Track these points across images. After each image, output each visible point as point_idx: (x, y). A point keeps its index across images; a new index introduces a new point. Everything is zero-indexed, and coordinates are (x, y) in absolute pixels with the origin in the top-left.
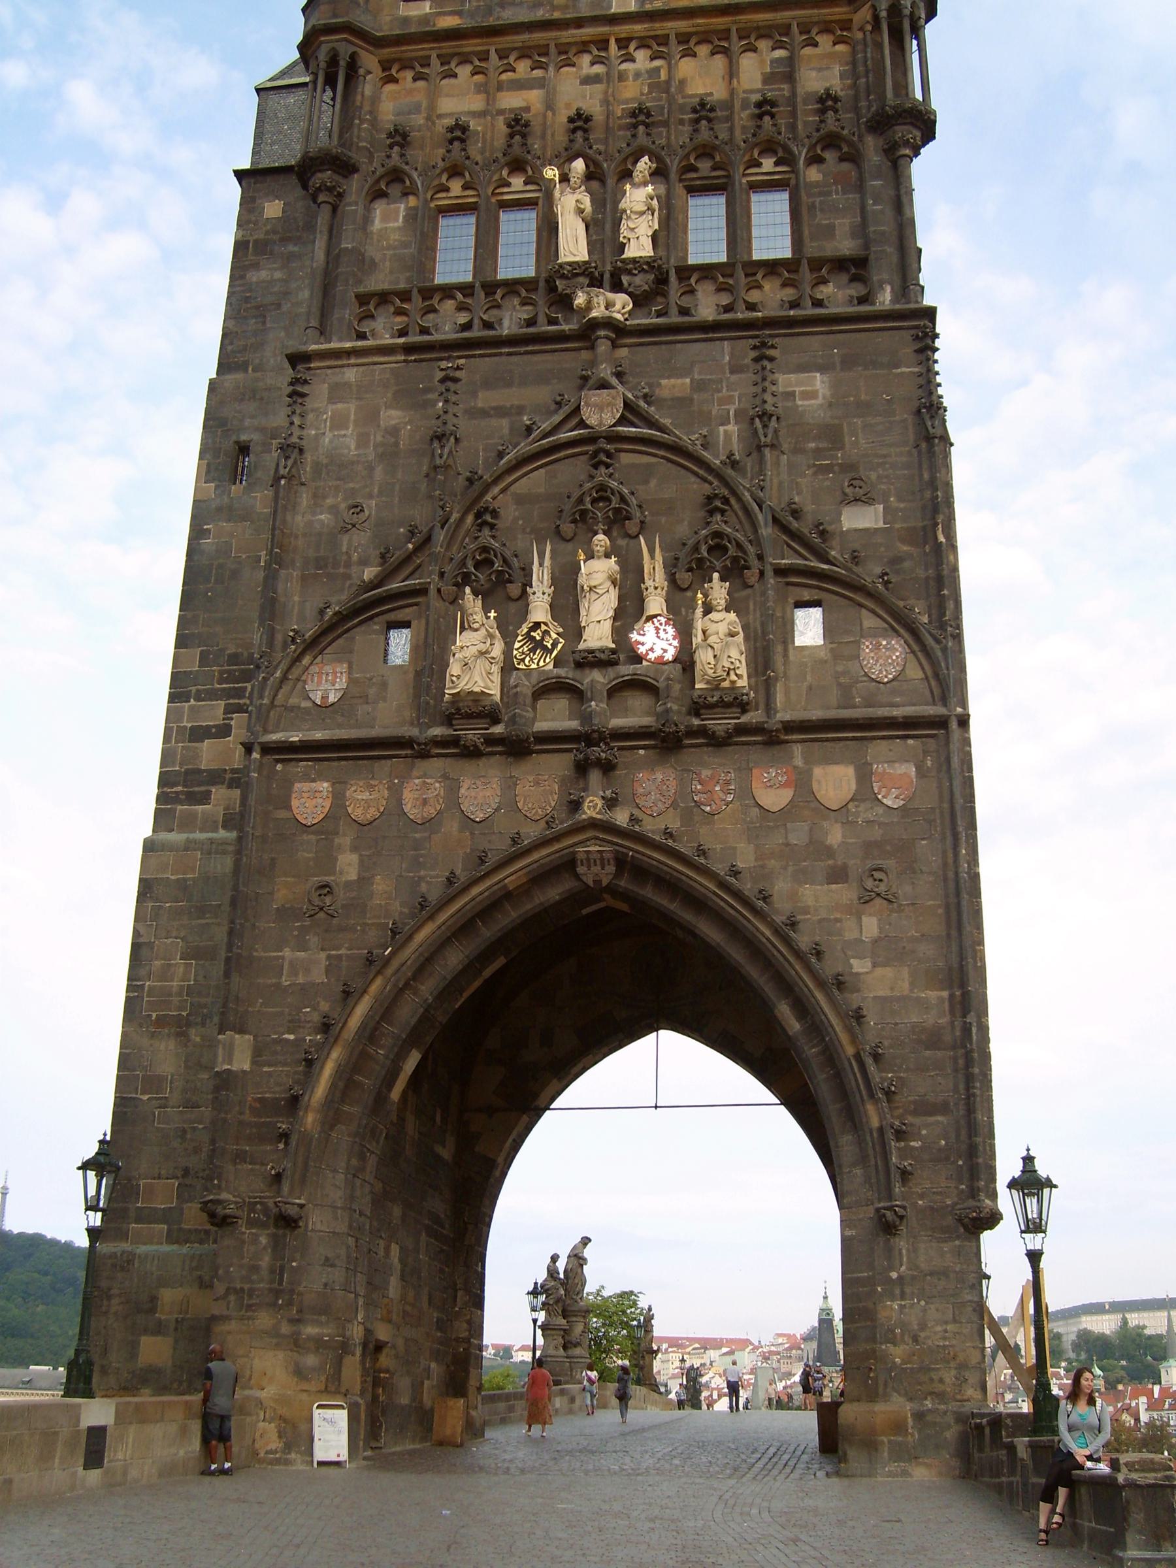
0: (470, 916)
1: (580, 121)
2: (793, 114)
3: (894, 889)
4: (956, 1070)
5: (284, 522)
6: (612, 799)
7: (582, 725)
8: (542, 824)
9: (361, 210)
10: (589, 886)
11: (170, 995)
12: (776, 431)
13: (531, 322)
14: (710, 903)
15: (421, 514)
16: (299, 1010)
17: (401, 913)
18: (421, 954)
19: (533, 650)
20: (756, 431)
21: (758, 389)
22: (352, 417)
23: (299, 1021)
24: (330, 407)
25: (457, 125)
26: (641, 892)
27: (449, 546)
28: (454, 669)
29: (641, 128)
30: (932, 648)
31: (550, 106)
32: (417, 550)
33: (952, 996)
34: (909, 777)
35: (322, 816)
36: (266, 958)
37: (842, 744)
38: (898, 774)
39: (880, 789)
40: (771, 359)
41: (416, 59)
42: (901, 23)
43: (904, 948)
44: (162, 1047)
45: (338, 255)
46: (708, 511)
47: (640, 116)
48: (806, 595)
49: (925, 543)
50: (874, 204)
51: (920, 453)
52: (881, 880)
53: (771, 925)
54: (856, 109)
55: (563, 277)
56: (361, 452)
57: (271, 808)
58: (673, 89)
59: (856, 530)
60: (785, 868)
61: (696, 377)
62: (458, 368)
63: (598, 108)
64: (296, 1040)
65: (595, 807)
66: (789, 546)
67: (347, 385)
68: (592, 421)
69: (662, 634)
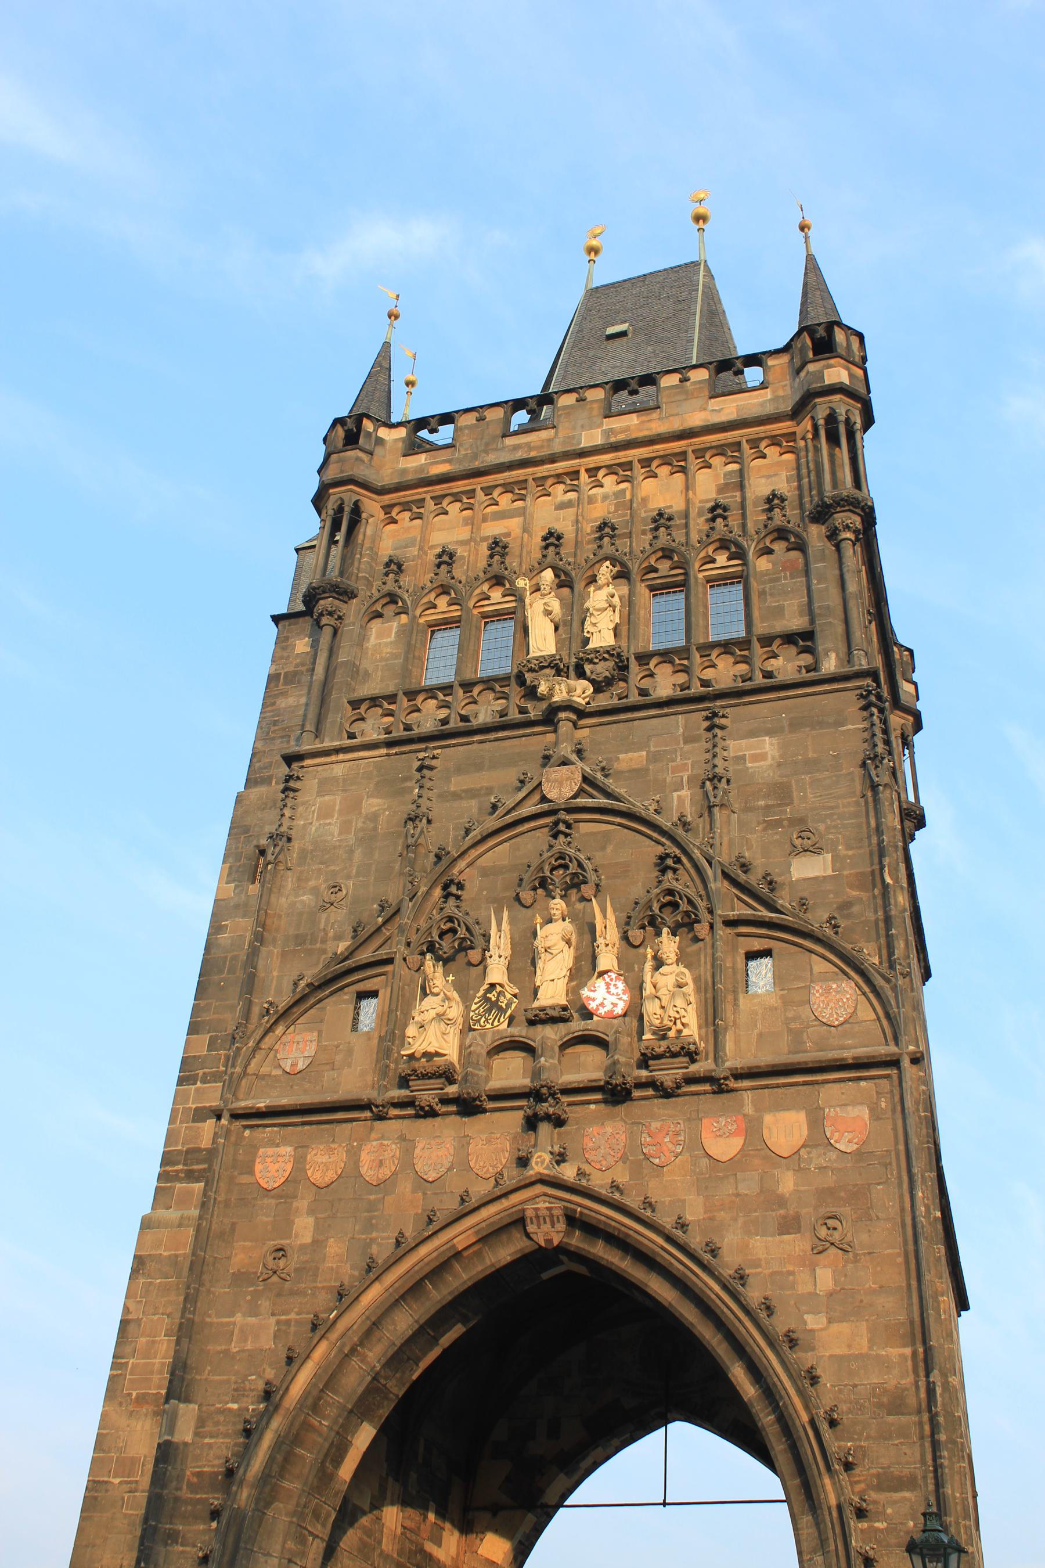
0: (418, 1278)
1: (552, 539)
2: (744, 516)
3: (849, 1238)
4: (922, 1438)
5: (268, 903)
6: (561, 1154)
7: (532, 1081)
8: (493, 1180)
9: (357, 629)
10: (540, 1247)
11: (152, 1373)
12: (726, 792)
13: (503, 714)
14: (658, 1259)
15: (393, 892)
16: (245, 1379)
17: (352, 1276)
18: (368, 1318)
19: (489, 1011)
20: (706, 795)
21: (709, 756)
22: (337, 807)
23: (245, 1390)
24: (319, 799)
25: (444, 551)
26: (592, 1250)
27: (415, 918)
28: (411, 1031)
29: (606, 540)
30: (882, 987)
31: (526, 529)
32: (385, 923)
33: (914, 1354)
34: (863, 1120)
35: (283, 1180)
36: (218, 1323)
37: (793, 1089)
38: (852, 1115)
39: (832, 1134)
40: (722, 728)
41: (412, 502)
42: (837, 429)
43: (861, 1301)
44: (139, 1428)
45: (336, 668)
46: (659, 871)
47: (605, 528)
48: (757, 945)
49: (874, 886)
50: (818, 584)
51: (866, 802)
52: (835, 1229)
53: (717, 1279)
54: (801, 505)
55: (531, 670)
56: (343, 837)
57: (236, 1173)
58: (635, 505)
59: (805, 880)
60: (735, 1220)
61: (652, 749)
62: (434, 757)
63: (570, 528)
64: (239, 1409)
65: (543, 1162)
66: (739, 899)
67: (335, 779)
68: (551, 793)
69: (612, 989)
